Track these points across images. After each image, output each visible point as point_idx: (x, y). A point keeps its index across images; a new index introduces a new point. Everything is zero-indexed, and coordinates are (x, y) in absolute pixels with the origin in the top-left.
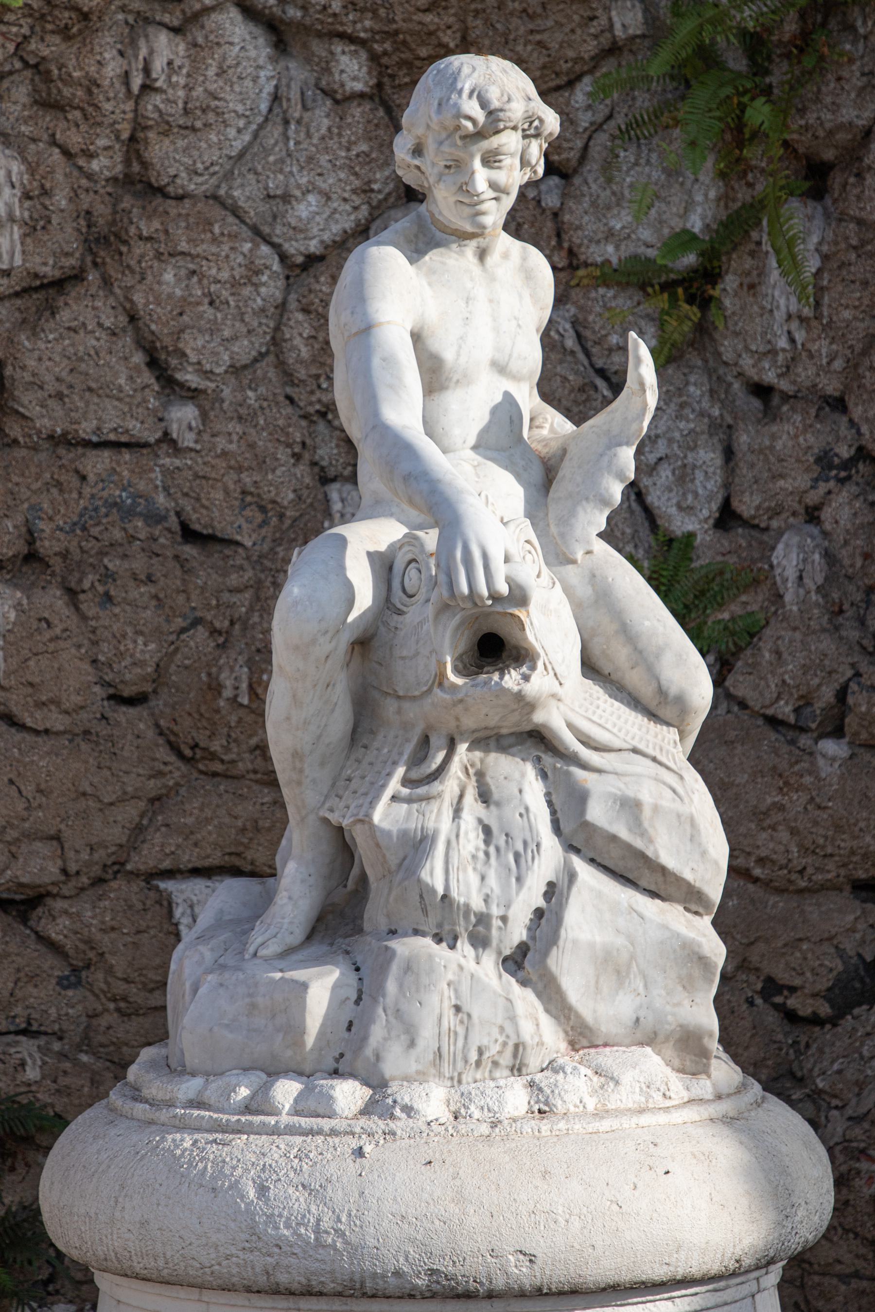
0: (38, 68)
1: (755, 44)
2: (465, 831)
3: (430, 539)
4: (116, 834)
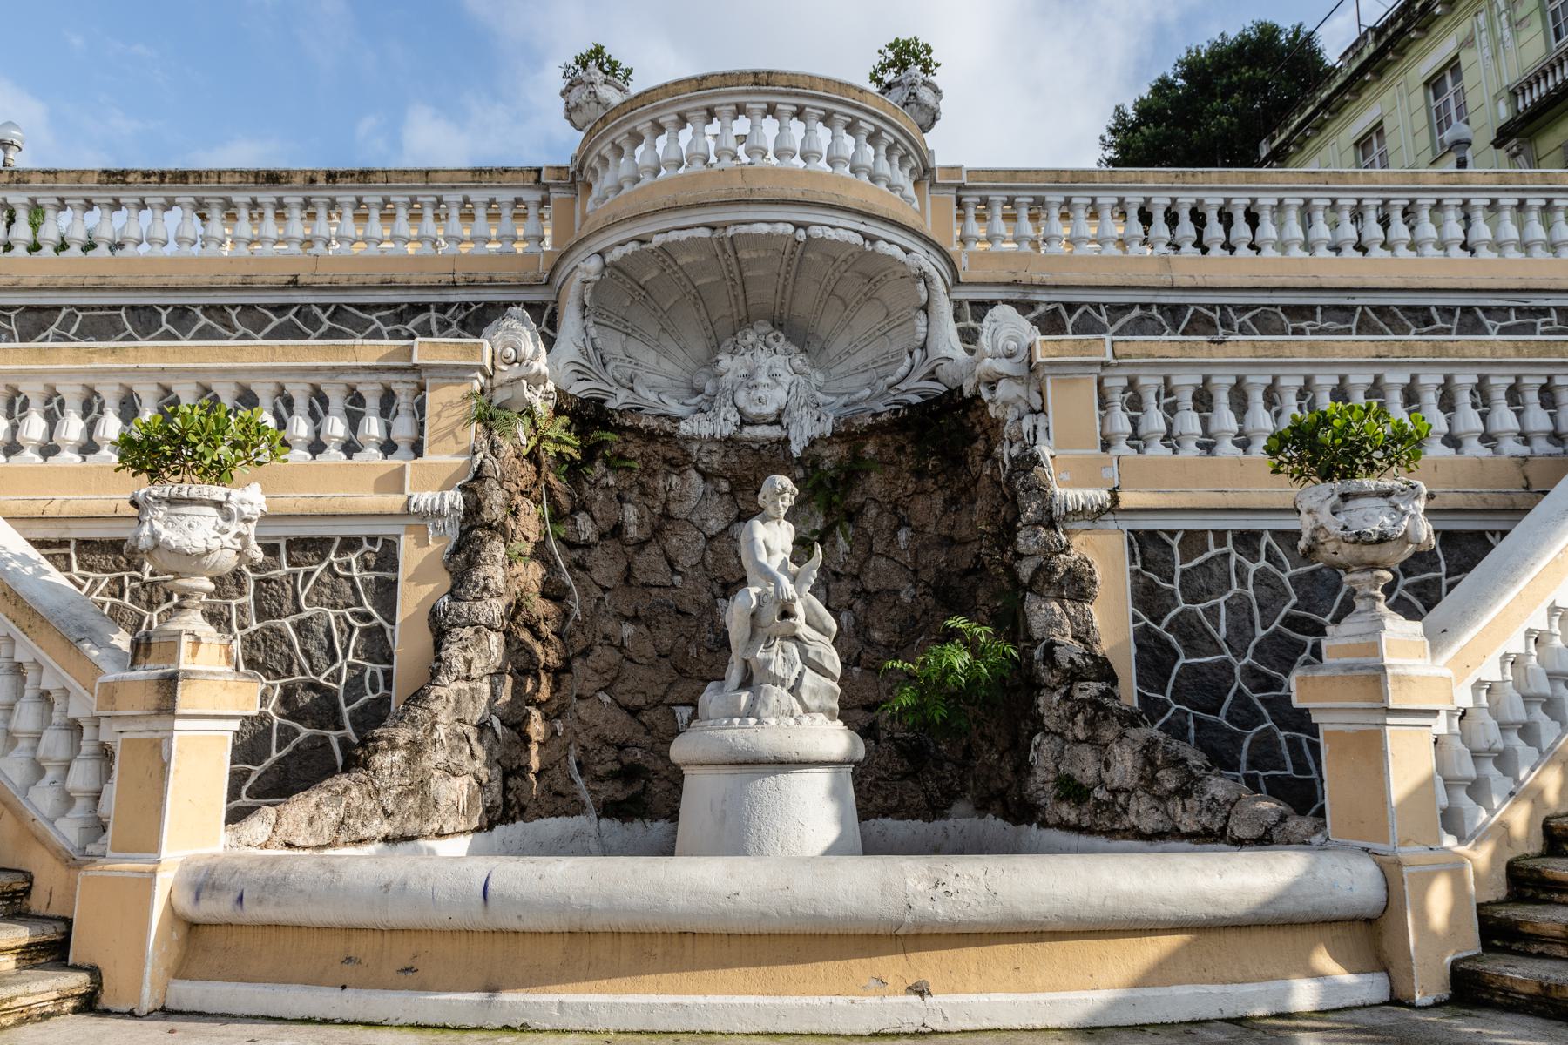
0: (642, 485)
1: (834, 481)
2: (779, 660)
3: (771, 589)
4: (660, 693)
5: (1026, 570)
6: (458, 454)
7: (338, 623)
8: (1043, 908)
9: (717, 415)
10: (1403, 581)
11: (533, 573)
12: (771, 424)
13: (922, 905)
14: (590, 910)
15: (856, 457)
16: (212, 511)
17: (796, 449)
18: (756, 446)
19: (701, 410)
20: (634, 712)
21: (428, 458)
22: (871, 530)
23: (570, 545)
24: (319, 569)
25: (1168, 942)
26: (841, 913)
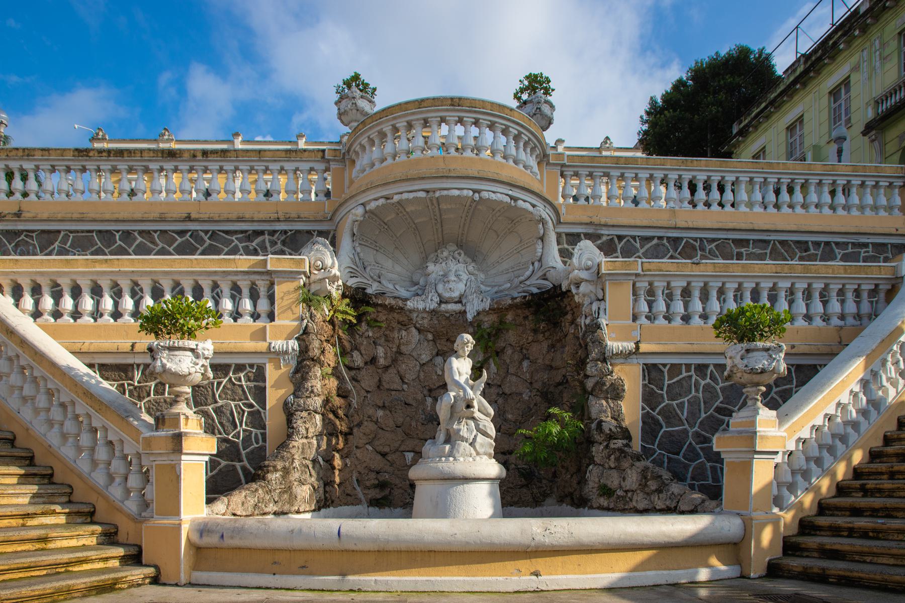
0: (386, 336)
1: (489, 334)
5: (590, 384)
6: (294, 320)
7: (236, 409)
8: (593, 539)
9: (427, 297)
10: (775, 390)
11: (333, 383)
12: (456, 303)
13: (539, 538)
14: (388, 541)
15: (501, 322)
16: (189, 353)
17: (470, 317)
18: (447, 315)
19: (418, 295)
20: (384, 455)
21: (277, 322)
22: (508, 361)
23: (349, 368)
24: (225, 381)
25: (646, 554)
26: (502, 542)
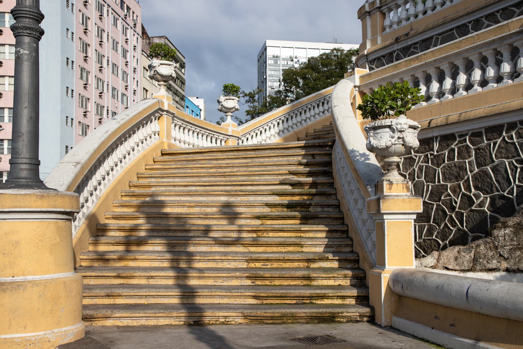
7: (510, 166)
24: (499, 141)
